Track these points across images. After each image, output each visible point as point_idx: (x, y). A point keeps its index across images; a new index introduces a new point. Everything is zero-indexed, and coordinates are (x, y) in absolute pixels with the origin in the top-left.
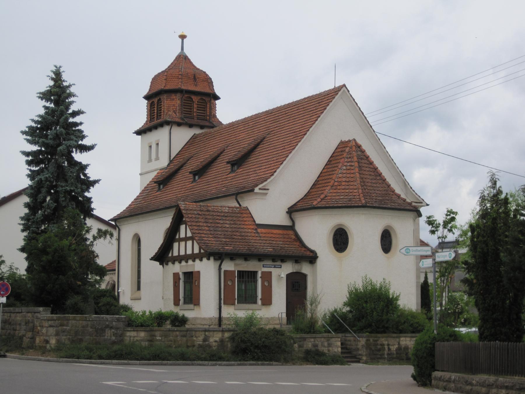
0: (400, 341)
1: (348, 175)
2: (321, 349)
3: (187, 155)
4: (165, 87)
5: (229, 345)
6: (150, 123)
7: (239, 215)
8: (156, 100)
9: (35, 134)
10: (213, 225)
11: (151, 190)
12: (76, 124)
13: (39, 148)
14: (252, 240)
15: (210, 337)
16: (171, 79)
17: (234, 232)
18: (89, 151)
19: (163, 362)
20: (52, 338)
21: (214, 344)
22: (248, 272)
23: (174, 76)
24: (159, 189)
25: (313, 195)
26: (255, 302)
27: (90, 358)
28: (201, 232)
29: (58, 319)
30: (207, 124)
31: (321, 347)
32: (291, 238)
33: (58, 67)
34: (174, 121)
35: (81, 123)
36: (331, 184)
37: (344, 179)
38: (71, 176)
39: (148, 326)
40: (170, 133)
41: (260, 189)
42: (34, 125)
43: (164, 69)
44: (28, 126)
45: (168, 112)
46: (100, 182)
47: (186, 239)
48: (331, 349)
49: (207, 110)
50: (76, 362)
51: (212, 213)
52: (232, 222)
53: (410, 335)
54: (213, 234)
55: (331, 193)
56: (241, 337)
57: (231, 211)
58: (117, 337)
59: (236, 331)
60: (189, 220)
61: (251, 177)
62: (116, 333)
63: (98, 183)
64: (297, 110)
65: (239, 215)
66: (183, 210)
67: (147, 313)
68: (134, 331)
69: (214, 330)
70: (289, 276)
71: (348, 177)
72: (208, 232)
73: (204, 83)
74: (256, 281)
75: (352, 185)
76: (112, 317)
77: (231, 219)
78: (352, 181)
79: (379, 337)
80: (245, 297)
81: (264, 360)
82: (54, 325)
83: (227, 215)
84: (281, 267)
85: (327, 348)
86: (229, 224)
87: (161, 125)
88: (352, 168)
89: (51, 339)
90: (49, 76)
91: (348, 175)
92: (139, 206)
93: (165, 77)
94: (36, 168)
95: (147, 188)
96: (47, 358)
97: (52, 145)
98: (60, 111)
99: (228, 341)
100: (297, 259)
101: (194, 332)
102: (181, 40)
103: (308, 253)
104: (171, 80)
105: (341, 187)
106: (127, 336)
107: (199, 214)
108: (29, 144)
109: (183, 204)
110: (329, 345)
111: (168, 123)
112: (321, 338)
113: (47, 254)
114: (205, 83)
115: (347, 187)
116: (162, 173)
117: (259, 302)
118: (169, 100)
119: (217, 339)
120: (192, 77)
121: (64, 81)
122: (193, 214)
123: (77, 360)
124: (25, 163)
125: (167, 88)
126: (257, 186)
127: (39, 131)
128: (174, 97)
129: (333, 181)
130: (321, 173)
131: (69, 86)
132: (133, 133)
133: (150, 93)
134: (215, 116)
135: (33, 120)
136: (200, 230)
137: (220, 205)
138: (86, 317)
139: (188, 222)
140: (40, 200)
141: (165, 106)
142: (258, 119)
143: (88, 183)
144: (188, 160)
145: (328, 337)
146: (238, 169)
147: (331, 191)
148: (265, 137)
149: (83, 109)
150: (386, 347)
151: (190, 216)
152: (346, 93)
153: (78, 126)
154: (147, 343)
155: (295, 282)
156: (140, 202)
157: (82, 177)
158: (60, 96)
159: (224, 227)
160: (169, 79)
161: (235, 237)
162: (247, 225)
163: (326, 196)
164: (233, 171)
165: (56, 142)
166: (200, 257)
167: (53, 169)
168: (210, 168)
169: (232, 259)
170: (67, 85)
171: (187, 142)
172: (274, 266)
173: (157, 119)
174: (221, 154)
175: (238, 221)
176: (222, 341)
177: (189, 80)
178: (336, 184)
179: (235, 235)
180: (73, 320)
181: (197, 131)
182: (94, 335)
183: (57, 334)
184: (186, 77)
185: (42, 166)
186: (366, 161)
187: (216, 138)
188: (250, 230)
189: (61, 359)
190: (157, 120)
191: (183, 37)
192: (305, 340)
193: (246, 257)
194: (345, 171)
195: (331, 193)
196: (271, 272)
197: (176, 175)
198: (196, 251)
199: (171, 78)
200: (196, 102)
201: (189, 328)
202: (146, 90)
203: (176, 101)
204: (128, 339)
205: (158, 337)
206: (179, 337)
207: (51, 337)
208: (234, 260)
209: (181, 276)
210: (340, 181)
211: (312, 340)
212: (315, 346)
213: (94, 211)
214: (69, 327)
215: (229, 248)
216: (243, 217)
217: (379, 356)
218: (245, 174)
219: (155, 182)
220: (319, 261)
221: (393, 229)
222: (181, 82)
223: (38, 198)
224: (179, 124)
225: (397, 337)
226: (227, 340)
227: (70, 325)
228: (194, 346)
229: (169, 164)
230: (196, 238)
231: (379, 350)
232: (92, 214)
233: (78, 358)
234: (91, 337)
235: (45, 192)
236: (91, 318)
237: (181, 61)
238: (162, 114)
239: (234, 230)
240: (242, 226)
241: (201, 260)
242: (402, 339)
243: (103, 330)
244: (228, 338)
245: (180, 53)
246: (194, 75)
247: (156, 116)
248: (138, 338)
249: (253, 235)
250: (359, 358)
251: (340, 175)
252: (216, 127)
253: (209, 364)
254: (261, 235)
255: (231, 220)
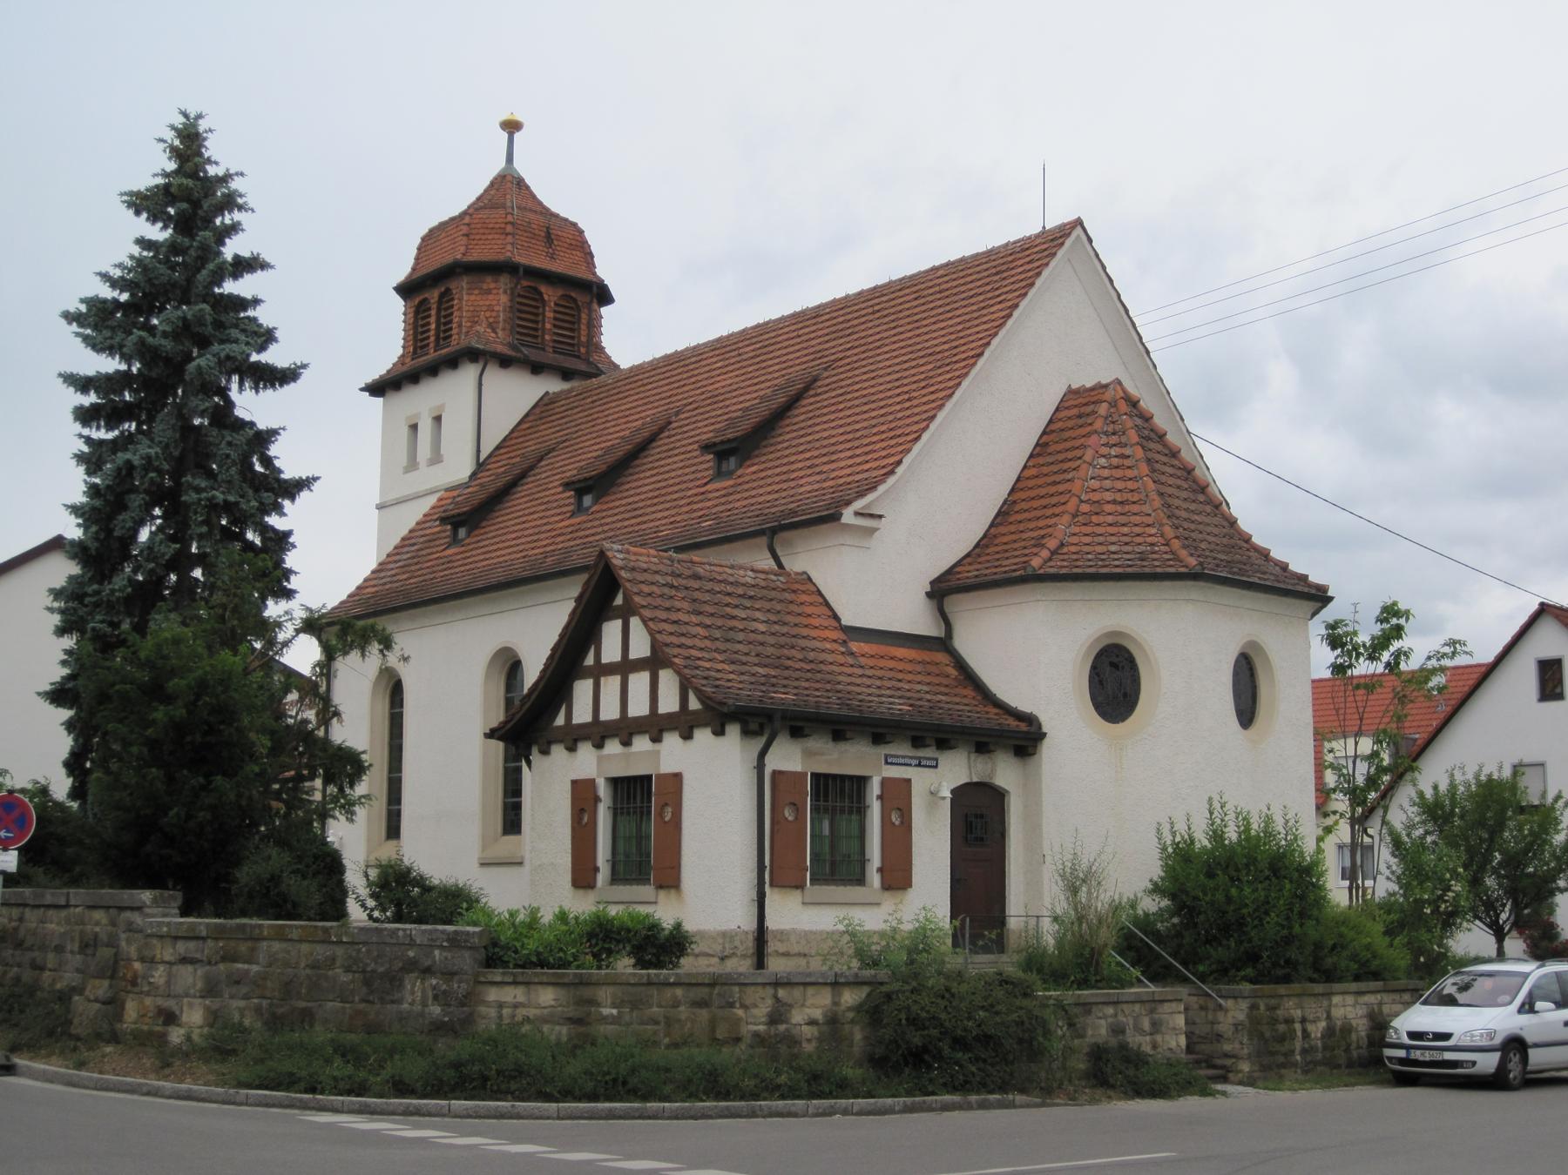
0: (1330, 1006)
1: (1120, 485)
2: (1136, 1040)
3: (532, 447)
4: (464, 255)
5: (858, 1036)
6: (413, 359)
7: (787, 596)
8: (433, 295)
9: (109, 323)
10: (719, 622)
11: (427, 545)
12: (241, 303)
13: (123, 367)
14: (840, 674)
15: (791, 1006)
16: (484, 234)
17: (782, 646)
18: (281, 386)
19: (649, 1105)
20: (191, 1005)
21: (808, 1031)
22: (843, 778)
23: (491, 226)
24: (455, 540)
25: (1005, 544)
26: (860, 880)
27: (360, 1090)
28: (689, 642)
29: (218, 934)
30: (583, 367)
31: (1134, 1036)
32: (948, 676)
33: (192, 116)
34: (492, 350)
35: (256, 302)
36: (1071, 507)
37: (1108, 496)
38: (228, 456)
39: (564, 964)
40: (480, 384)
41: (857, 514)
42: (107, 293)
43: (456, 212)
44: (86, 298)
45: (471, 327)
46: (316, 486)
47: (625, 667)
48: (1159, 1038)
49: (580, 329)
50: (305, 1106)
51: (709, 586)
52: (773, 618)
53: (1354, 986)
54: (725, 651)
55: (1074, 535)
56: (908, 1008)
57: (763, 584)
58: (450, 1005)
59: (882, 984)
60: (645, 604)
61: (802, 486)
62: (445, 992)
63: (309, 488)
64: (916, 299)
65: (787, 596)
66: (622, 568)
67: (547, 917)
68: (515, 983)
69: (808, 980)
70: (958, 793)
71: (1120, 491)
72: (707, 643)
73: (574, 252)
74: (861, 810)
75: (1135, 514)
76: (431, 932)
77: (767, 605)
78: (1134, 500)
79: (1282, 996)
80: (833, 863)
81: (983, 1087)
82: (198, 956)
83: (753, 593)
84: (936, 767)
85: (1148, 1038)
86: (764, 622)
87: (453, 362)
88: (1127, 462)
89: (185, 1008)
90: (165, 141)
91: (1120, 485)
92: (390, 588)
93: (465, 229)
94: (107, 431)
95: (409, 539)
96: (183, 1086)
97: (170, 355)
98: (199, 248)
99: (852, 1021)
100: (982, 743)
101: (736, 989)
102: (507, 135)
103: (1012, 723)
104: (483, 237)
105: (1101, 519)
106: (487, 1004)
107: (672, 586)
108: (89, 352)
109: (618, 551)
110: (1156, 1026)
111: (473, 355)
112: (1133, 1002)
113: (168, 699)
114: (578, 253)
115: (1122, 519)
116: (454, 497)
117: (875, 879)
118: (476, 292)
119: (817, 1014)
120: (543, 234)
121: (209, 161)
122: (652, 583)
123: (311, 1096)
124: (71, 417)
125: (475, 256)
126: (848, 503)
127: (122, 315)
128: (492, 285)
129: (1074, 500)
130: (1018, 480)
131: (225, 179)
132: (362, 390)
133: (414, 277)
134: (600, 349)
135: (105, 277)
136: (683, 635)
137: (729, 564)
138: (326, 930)
139: (643, 606)
140: (124, 531)
141: (465, 308)
142: (772, 334)
143: (276, 486)
144: (541, 459)
145: (1154, 1001)
146: (741, 466)
147: (1076, 530)
148: (818, 375)
149: (266, 256)
150: (1298, 1026)
151: (646, 589)
152: (1084, 246)
153: (245, 310)
154: (564, 1030)
155: (976, 816)
156: (395, 579)
157: (258, 468)
158: (196, 204)
159: (752, 631)
160: (478, 234)
161: (789, 663)
162: (816, 627)
163: (1062, 545)
164: (720, 474)
165: (181, 348)
166: (684, 725)
167: (169, 433)
168: (627, 472)
169: (797, 733)
170: (221, 174)
171: (527, 415)
172: (917, 762)
173: (437, 347)
174: (662, 432)
175: (789, 613)
176: (833, 1020)
177: (534, 241)
178: (1085, 508)
179: (789, 659)
180: (275, 940)
181: (554, 385)
182: (357, 998)
183: (210, 990)
184: (525, 231)
185: (130, 427)
186: (1159, 447)
187: (626, 397)
188: (828, 646)
189: (244, 1091)
190: (435, 351)
191: (512, 127)
192: (1089, 1012)
193: (840, 728)
194: (1106, 473)
195: (1074, 535)
196: (909, 781)
197: (506, 498)
198: (669, 703)
199: (481, 231)
200: (552, 304)
201: (720, 975)
202: (402, 270)
203: (497, 297)
204: (493, 1012)
205: (606, 1007)
206: (682, 1008)
207: (185, 1000)
208: (806, 736)
209: (603, 790)
210: (1098, 502)
211: (1110, 1010)
212: (1118, 1030)
213: (293, 578)
214: (258, 964)
215: (784, 697)
216: (802, 604)
217: (1281, 1059)
218: (777, 479)
219: (443, 520)
220: (1047, 749)
221: (1265, 654)
222: (512, 244)
223: (115, 526)
224: (505, 362)
225: (1323, 995)
226: (851, 1015)
227: (262, 957)
228: (738, 1040)
229: (473, 476)
230: (676, 660)
231: (1282, 1039)
232: (285, 587)
233: (312, 1090)
234: (348, 1005)
235: (140, 506)
236: (346, 933)
237: (509, 191)
238: (454, 331)
239: (783, 640)
240: (805, 632)
241: (687, 736)
242: (1336, 999)
243: (393, 980)
244: (858, 1009)
245: (504, 169)
246: (548, 228)
247: (432, 339)
248: (532, 1012)
249: (841, 659)
250: (1223, 1067)
251: (1094, 484)
252: (604, 373)
253: (810, 1112)
254: (863, 661)
255: (769, 611)
